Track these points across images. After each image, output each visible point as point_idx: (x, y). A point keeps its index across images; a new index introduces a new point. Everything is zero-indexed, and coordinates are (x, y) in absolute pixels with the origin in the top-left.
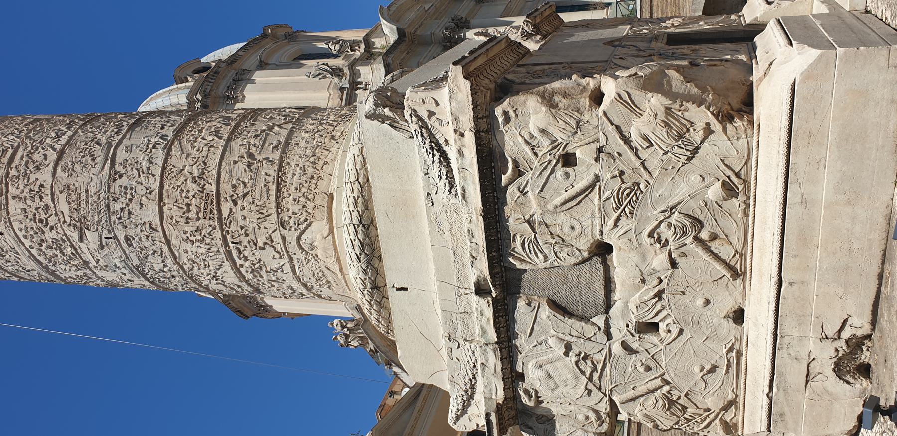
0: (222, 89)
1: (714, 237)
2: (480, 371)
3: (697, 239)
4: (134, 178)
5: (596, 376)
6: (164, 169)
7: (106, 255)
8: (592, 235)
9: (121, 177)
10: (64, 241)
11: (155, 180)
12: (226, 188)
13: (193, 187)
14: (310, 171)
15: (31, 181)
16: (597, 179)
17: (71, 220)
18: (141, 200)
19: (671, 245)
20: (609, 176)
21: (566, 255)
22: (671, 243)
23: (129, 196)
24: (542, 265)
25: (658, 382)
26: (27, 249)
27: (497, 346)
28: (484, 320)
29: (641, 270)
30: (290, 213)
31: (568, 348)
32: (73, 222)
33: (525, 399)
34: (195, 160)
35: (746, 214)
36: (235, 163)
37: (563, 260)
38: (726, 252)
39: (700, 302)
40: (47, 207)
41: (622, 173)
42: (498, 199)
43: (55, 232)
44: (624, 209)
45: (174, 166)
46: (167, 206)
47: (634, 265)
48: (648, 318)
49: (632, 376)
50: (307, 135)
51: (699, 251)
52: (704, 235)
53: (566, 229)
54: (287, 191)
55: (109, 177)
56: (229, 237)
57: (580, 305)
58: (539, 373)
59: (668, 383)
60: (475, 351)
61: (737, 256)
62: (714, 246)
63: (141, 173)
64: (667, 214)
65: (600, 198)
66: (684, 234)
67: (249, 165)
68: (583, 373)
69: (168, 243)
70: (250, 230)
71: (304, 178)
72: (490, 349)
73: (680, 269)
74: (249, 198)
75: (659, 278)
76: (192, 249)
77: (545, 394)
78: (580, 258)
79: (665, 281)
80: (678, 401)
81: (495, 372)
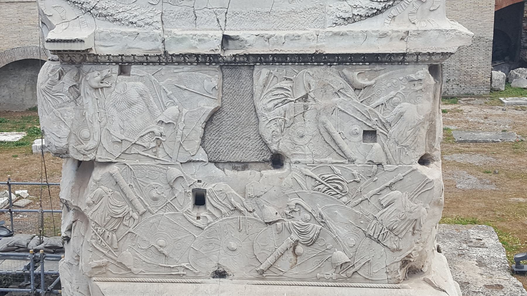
8: (295, 154)
21: (273, 129)
22: (291, 222)
24: (259, 105)
28: (194, 43)
37: (267, 126)
38: (284, 264)
39: (233, 245)
44: (322, 184)
47: (266, 190)
49: (144, 185)
53: (300, 130)
64: (319, 219)
65: (333, 164)
66: (301, 233)
78: (270, 142)
79: (251, 216)
80: (122, 225)
81: (130, 48)
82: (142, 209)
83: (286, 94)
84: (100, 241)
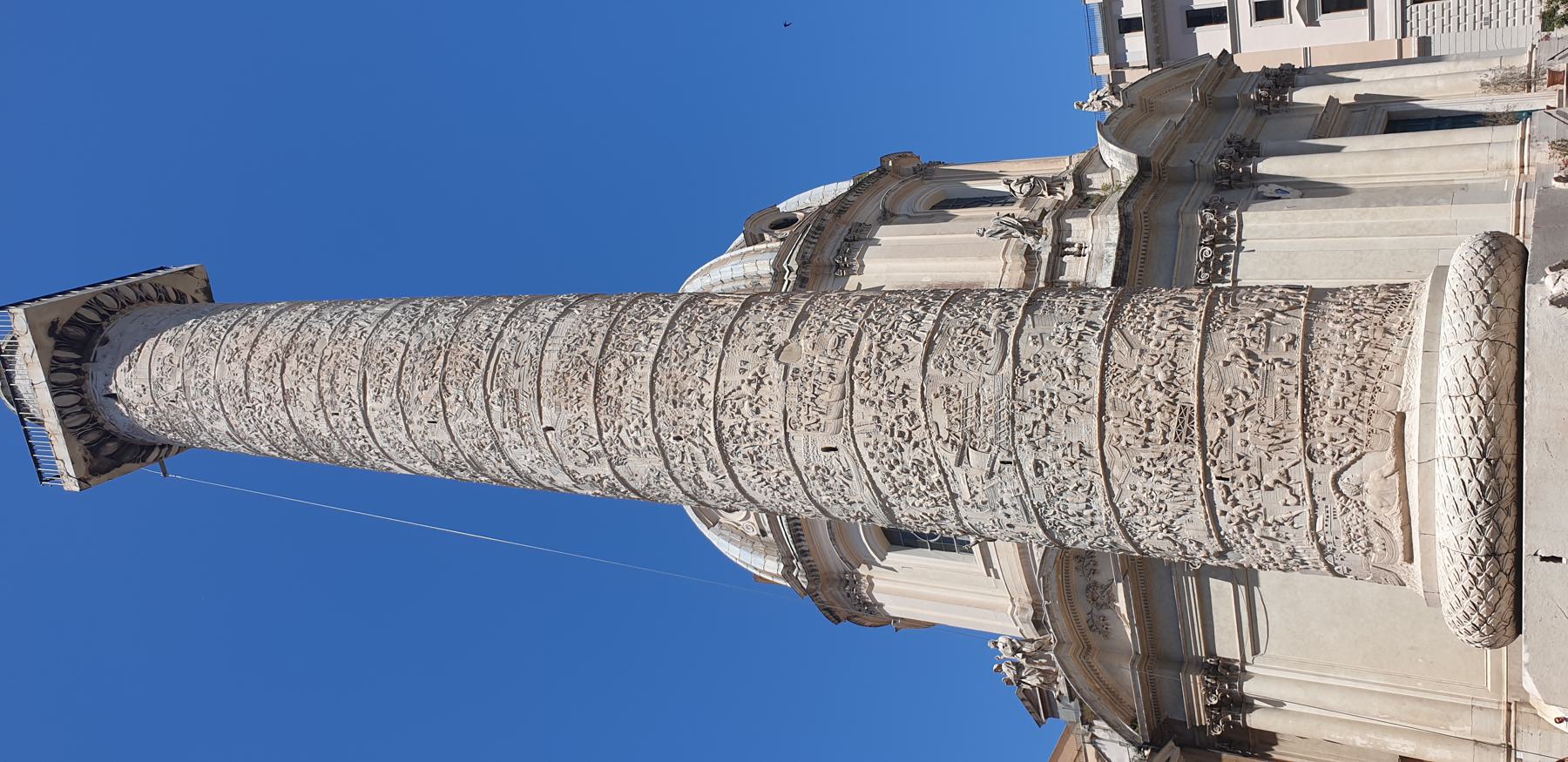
0: (828, 254)
4: (1054, 380)
6: (1104, 369)
7: (993, 486)
9: (1032, 378)
10: (931, 463)
11: (1091, 384)
12: (1214, 400)
13: (1158, 398)
14: (1359, 378)
15: (889, 379)
17: (950, 435)
18: (1067, 412)
23: (1047, 405)
26: (868, 473)
30: (1326, 439)
32: (954, 438)
34: (1156, 359)
36: (1226, 364)
40: (912, 413)
43: (920, 451)
45: (1119, 365)
46: (1111, 421)
50: (1338, 327)
54: (1321, 407)
55: (1014, 378)
56: (1214, 471)
63: (1066, 375)
67: (1252, 368)
69: (1107, 473)
70: (1253, 460)
71: (1351, 389)
74: (1254, 414)
76: (1145, 485)
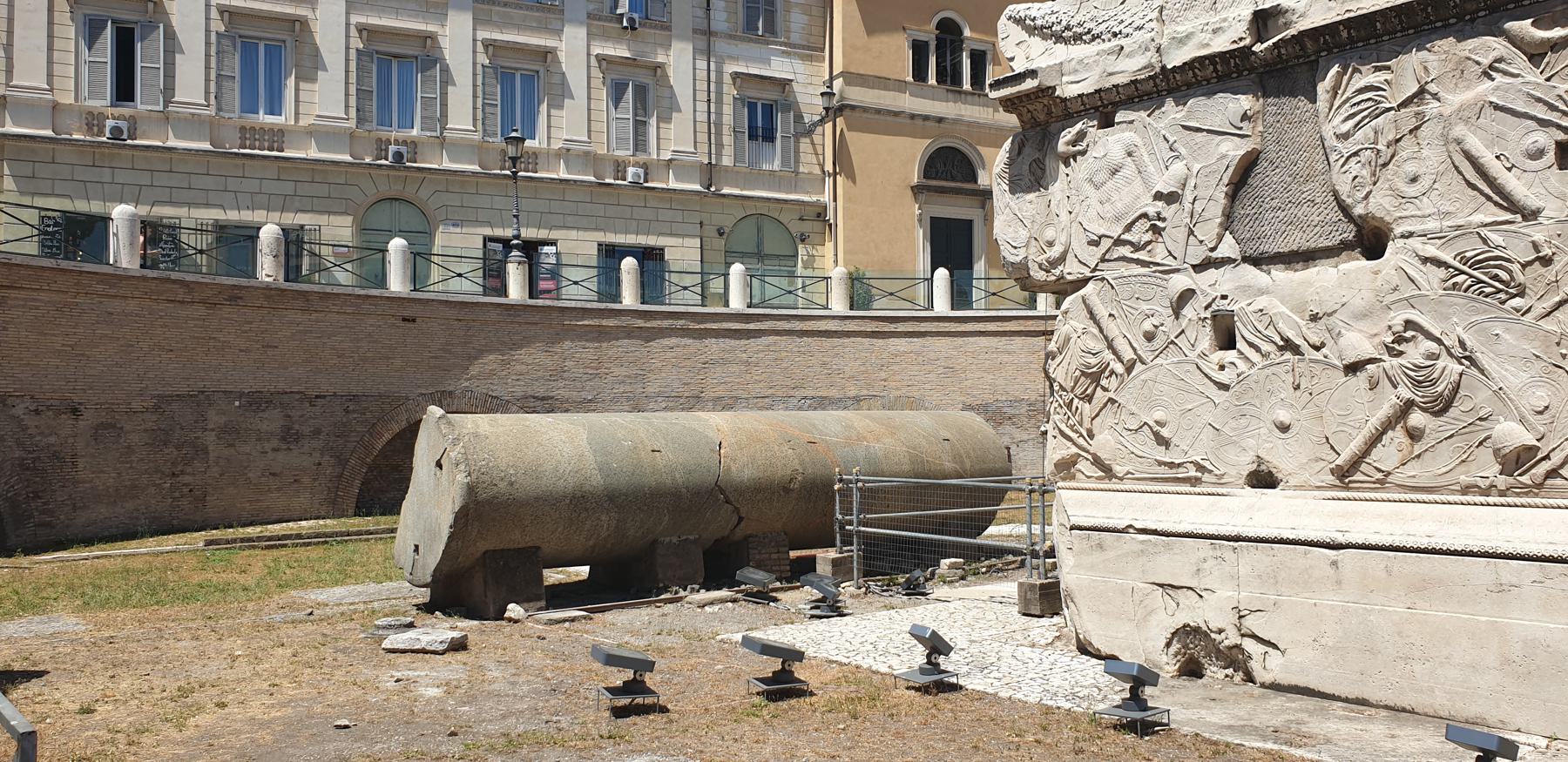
1: (1414, 435)
2: (1107, 45)
3: (1409, 405)
5: (1125, 251)
8: (1400, 218)
16: (1531, 215)
19: (1390, 363)
20: (1539, 237)
21: (1354, 174)
22: (1395, 361)
24: (1328, 131)
25: (1128, 355)
27: (1158, 70)
28: (1204, 37)
29: (1335, 312)
31: (1171, 198)
33: (1068, 134)
35: (1466, 490)
38: (1387, 455)
39: (1284, 416)
41: (1546, 261)
42: (1472, 20)
44: (1463, 272)
47: (1344, 300)
48: (1242, 330)
49: (1133, 311)
51: (1385, 410)
52: (1417, 418)
53: (1411, 168)
57: (1254, 211)
58: (1117, 154)
59: (1129, 369)
60: (1143, 31)
61: (1379, 476)
62: (1397, 435)
64: (1458, 351)
65: (1486, 225)
66: (1418, 384)
68: (1128, 228)
72: (1150, 57)
73: (1345, 379)
75: (1323, 345)
77: (1081, 168)
78: (1349, 201)
79: (1318, 356)
80: (1099, 388)
81: (1110, 74)
82: (1128, 355)
83: (1376, 98)
84: (1066, 417)
